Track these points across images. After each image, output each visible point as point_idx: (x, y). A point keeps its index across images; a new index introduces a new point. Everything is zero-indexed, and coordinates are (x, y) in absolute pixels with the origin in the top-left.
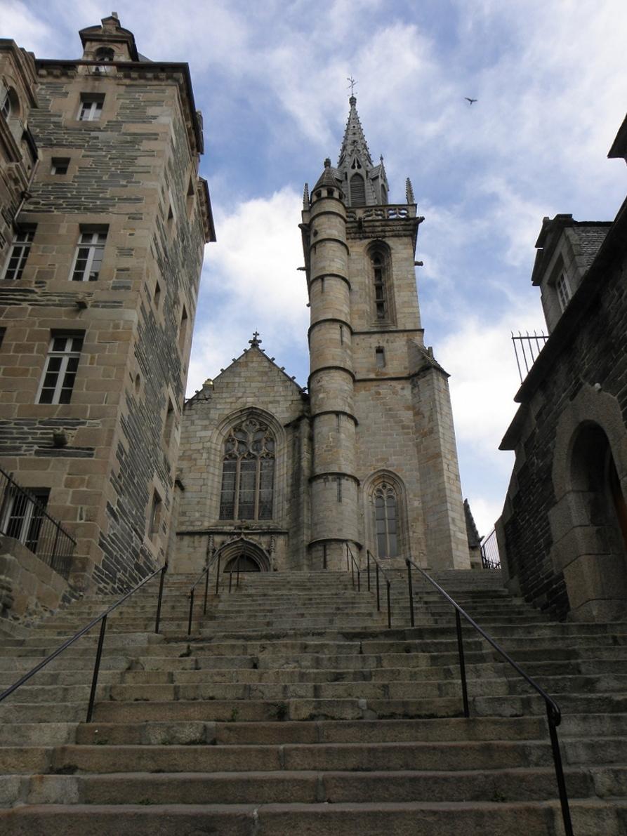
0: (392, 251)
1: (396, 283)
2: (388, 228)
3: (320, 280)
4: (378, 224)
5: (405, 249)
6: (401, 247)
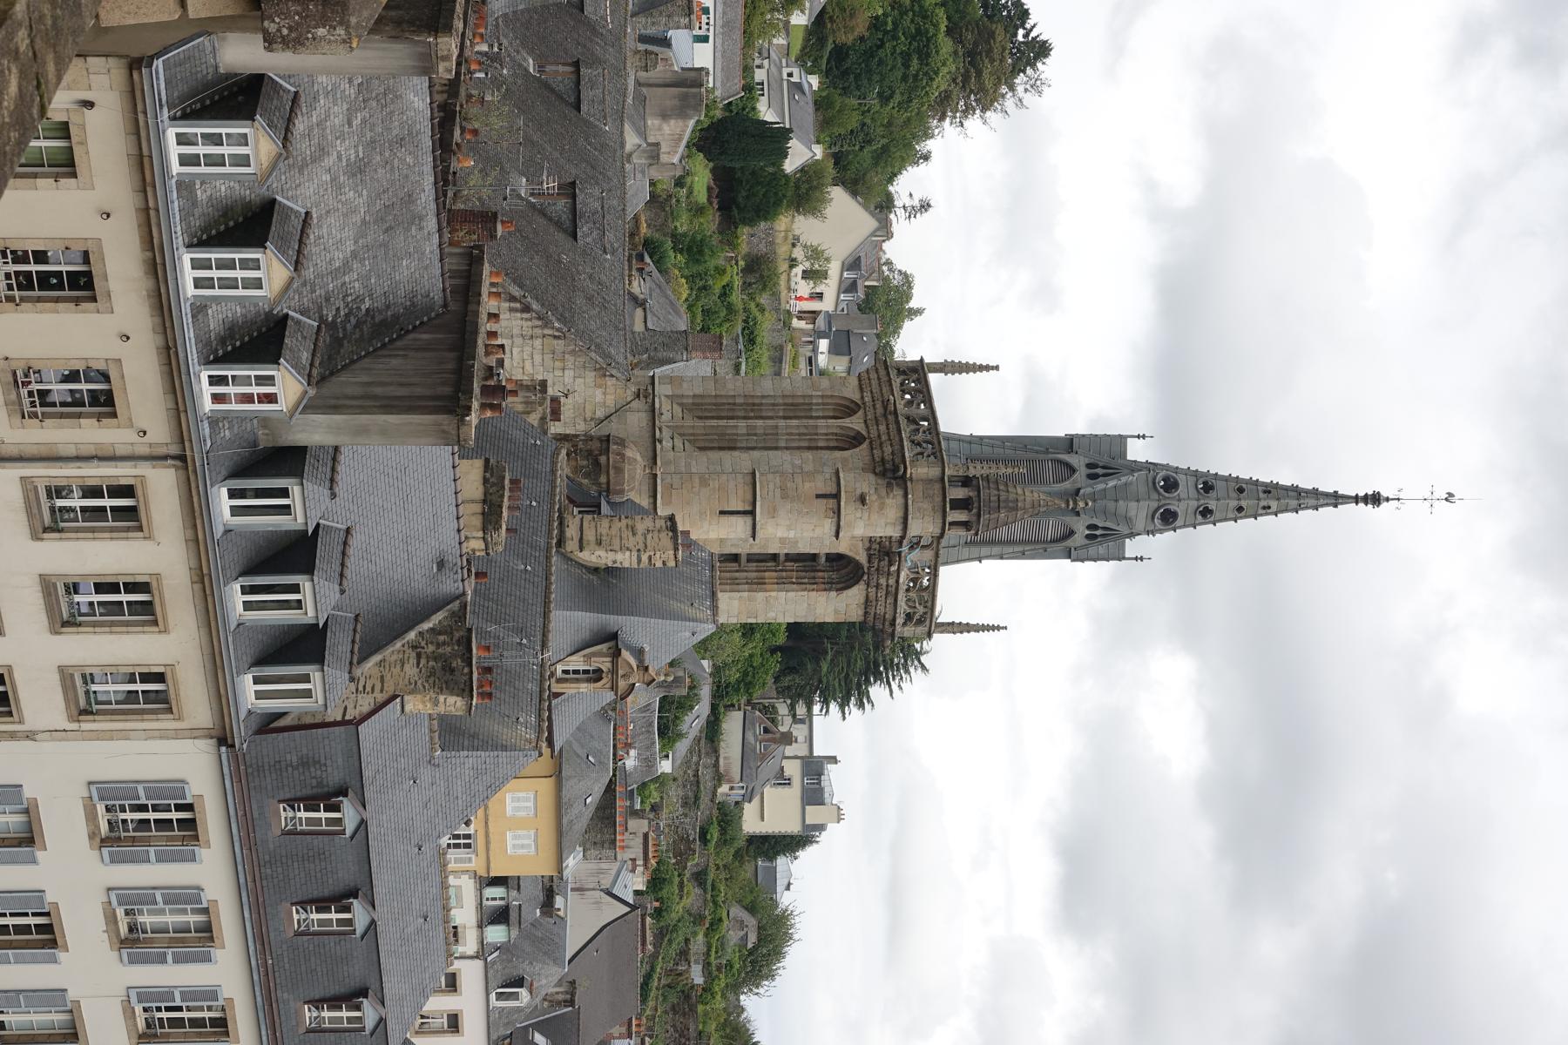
0: (833, 594)
1: (760, 596)
2: (882, 593)
3: (748, 508)
4: (892, 582)
5: (836, 612)
6: (842, 607)
